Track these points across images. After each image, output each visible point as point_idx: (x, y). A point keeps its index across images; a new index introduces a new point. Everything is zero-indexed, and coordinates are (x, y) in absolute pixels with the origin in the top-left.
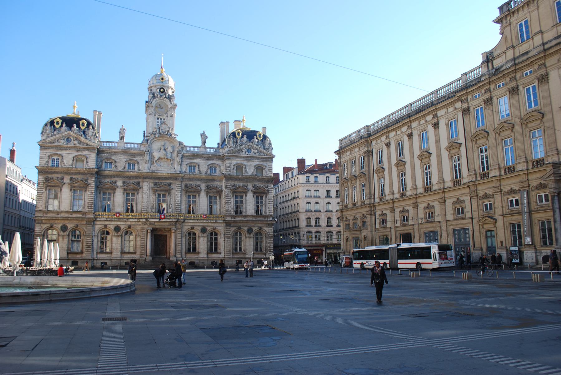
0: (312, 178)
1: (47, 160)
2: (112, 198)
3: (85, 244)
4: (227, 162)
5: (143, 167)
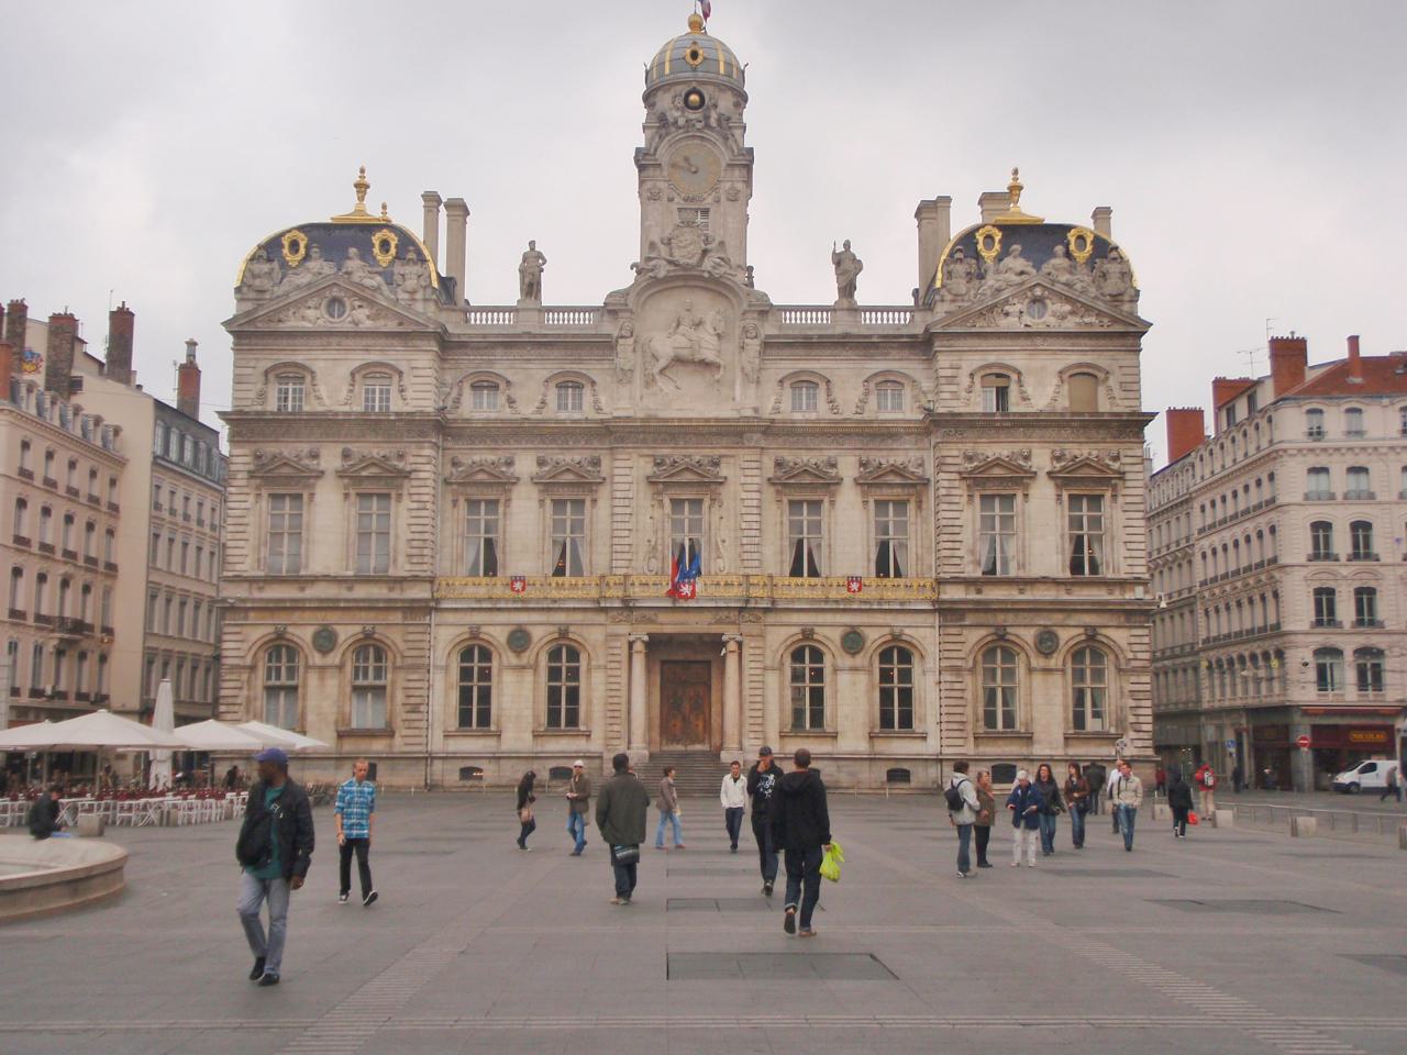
0: (1335, 420)
1: (260, 386)
2: (501, 523)
3: (400, 697)
4: (944, 361)
5: (614, 400)
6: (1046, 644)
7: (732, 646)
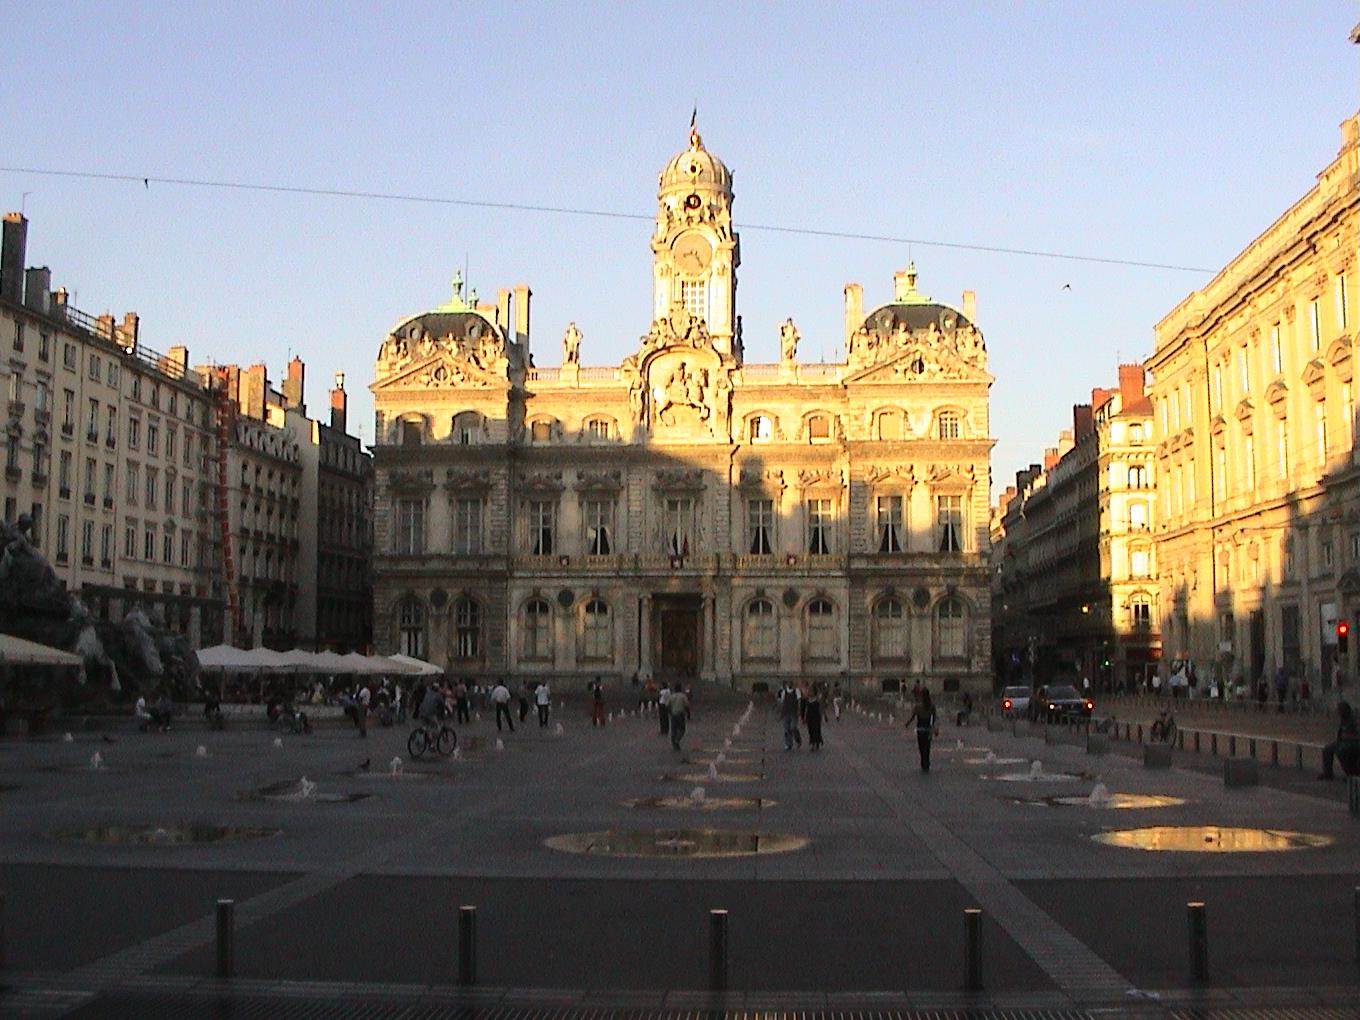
6: (922, 597)
7: (709, 602)
